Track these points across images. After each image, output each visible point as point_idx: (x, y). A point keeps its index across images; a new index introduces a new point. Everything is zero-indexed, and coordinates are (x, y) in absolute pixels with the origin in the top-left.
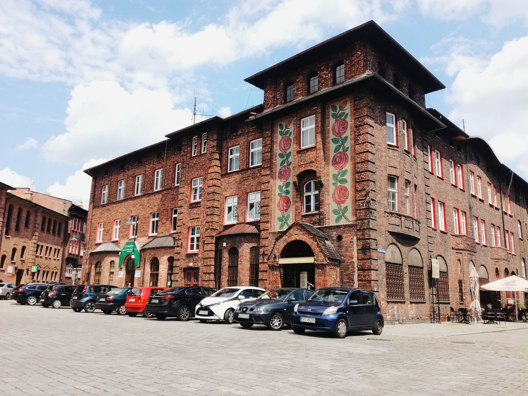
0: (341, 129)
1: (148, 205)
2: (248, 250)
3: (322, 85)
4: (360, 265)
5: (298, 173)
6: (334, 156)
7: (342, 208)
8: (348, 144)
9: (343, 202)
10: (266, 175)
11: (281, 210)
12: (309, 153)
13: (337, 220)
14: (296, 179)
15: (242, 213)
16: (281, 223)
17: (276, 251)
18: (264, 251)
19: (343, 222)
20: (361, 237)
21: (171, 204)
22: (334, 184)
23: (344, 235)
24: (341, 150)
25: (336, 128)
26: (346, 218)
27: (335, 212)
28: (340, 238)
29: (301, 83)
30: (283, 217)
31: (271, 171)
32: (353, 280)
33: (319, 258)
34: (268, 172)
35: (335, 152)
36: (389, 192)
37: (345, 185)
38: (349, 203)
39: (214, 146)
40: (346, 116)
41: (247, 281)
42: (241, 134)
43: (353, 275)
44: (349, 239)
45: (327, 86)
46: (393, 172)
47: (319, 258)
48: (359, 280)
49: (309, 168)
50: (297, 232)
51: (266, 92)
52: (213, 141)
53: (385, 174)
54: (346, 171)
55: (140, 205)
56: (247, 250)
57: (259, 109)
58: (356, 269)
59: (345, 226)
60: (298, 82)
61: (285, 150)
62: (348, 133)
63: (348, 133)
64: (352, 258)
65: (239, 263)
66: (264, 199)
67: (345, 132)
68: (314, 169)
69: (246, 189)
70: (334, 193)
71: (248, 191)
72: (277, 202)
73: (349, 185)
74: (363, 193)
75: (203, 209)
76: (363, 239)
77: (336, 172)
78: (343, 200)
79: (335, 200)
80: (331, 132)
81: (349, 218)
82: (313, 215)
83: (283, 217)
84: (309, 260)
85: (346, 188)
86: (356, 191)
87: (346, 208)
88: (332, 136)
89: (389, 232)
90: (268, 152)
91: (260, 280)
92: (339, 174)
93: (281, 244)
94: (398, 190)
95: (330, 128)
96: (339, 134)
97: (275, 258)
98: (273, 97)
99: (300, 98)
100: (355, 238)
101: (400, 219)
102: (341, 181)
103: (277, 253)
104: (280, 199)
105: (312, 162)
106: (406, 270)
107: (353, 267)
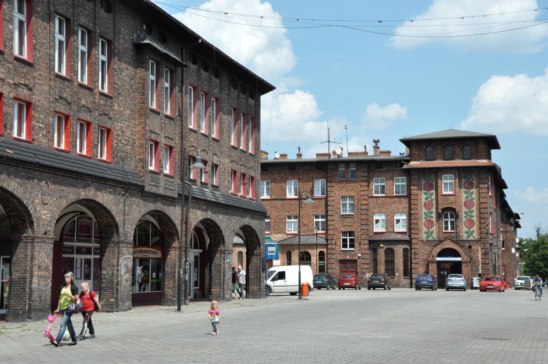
1: (282, 208)
2: (402, 250)
8: (474, 196)
9: (472, 228)
11: (427, 228)
12: (450, 197)
13: (468, 237)
14: (440, 211)
19: (471, 238)
21: (313, 211)
23: (473, 246)
24: (470, 198)
27: (466, 232)
28: (470, 247)
35: (466, 198)
37: (473, 219)
38: (475, 228)
39: (364, 176)
40: (473, 179)
44: (476, 248)
49: (451, 206)
52: (363, 172)
55: (271, 207)
58: (480, 263)
68: (454, 207)
72: (423, 222)
73: (475, 219)
74: (485, 225)
75: (355, 220)
77: (467, 210)
79: (466, 226)
81: (476, 236)
84: (459, 259)
86: (480, 223)
93: (438, 249)
97: (433, 257)
98: (418, 154)
100: (480, 248)
102: (470, 216)
107: (479, 262)
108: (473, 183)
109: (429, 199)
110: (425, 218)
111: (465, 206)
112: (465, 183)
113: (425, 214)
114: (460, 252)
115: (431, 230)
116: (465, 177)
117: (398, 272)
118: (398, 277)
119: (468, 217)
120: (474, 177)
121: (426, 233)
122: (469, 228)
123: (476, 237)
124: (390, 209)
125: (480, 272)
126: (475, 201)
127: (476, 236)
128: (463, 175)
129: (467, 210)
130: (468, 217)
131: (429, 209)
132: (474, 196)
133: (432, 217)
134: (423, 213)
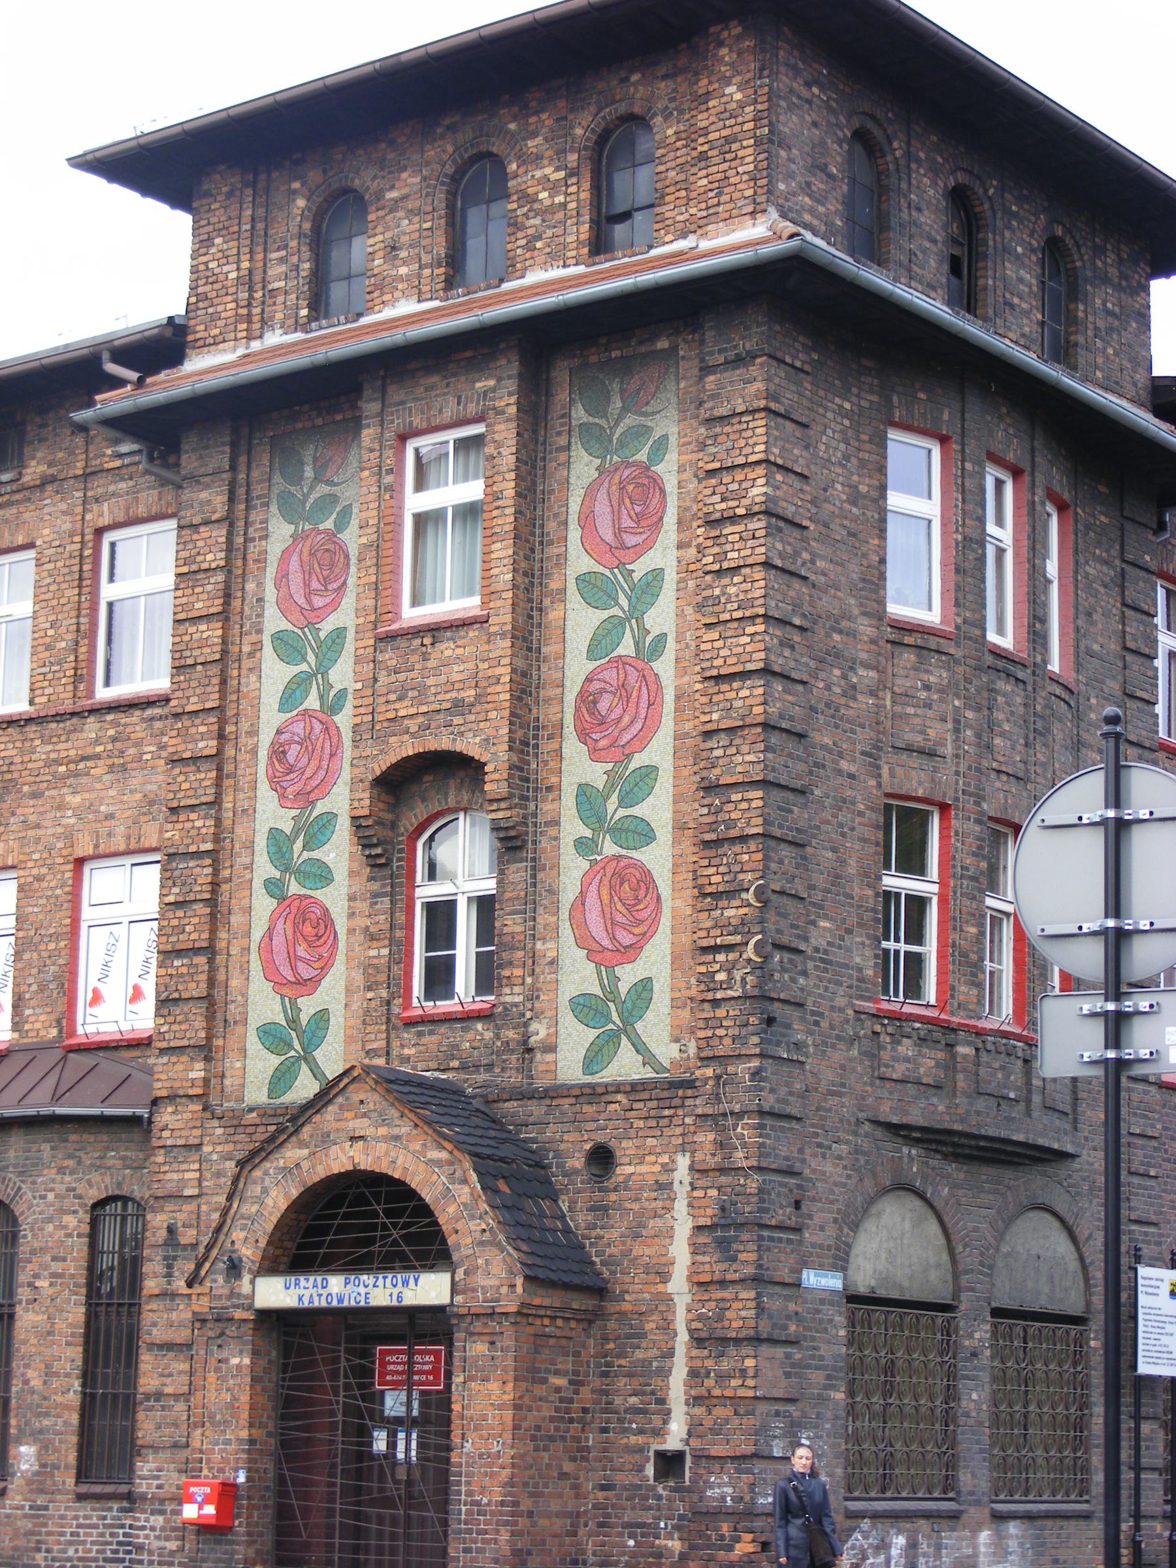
0: (627, 522)
3: (530, 247)
4: (700, 1318)
5: (379, 766)
6: (589, 680)
7: (623, 987)
8: (662, 616)
9: (630, 952)
10: (194, 759)
12: (447, 649)
13: (595, 1057)
15: (42, 988)
16: (276, 1060)
17: (238, 1235)
18: (171, 1230)
19: (625, 1065)
20: (712, 1162)
22: (581, 845)
23: (625, 1148)
24: (626, 647)
25: (602, 508)
26: (639, 1047)
28: (602, 1158)
29: (411, 212)
30: (293, 1022)
31: (221, 736)
32: (662, 1401)
33: (481, 1280)
34: (208, 746)
35: (591, 654)
36: (889, 896)
38: (656, 961)
40: (661, 446)
41: (67, 1407)
42: (46, 481)
43: (665, 1373)
44: (648, 1169)
45: (557, 256)
46: (915, 780)
47: (481, 1280)
48: (695, 1401)
49: (443, 742)
50: (360, 1125)
51: (202, 243)
53: (865, 796)
54: (650, 772)
56: (70, 1221)
57: (161, 348)
58: (683, 1337)
59: (635, 1088)
60: (395, 205)
61: (311, 616)
62: (663, 555)
63: (663, 555)
64: (665, 1277)
65: (23, 1293)
66: (177, 904)
67: (648, 545)
68: (470, 745)
69: (69, 837)
70: (583, 894)
71: (84, 847)
72: (257, 934)
73: (659, 858)
76: (722, 1171)
77: (596, 774)
78: (626, 939)
79: (584, 940)
80: (574, 534)
82: (468, 1018)
83: (293, 1022)
84: (429, 1289)
85: (647, 874)
87: (644, 987)
88: (579, 562)
89: (876, 1123)
90: (207, 617)
91: (148, 1396)
92: (610, 786)
93: (273, 1195)
94: (942, 883)
95: (575, 505)
96: (618, 553)
97: (234, 1268)
98: (248, 282)
99: (407, 307)
100: (683, 1162)
101: (950, 1046)
103: (247, 1243)
104: (273, 921)
105: (458, 706)
106: (978, 1334)
107: (667, 1327)
108: (656, 484)
109: (312, 702)
110: (269, 884)
111: (583, 735)
112: (590, 492)
113: (279, 843)
114: (446, 1215)
115: (308, 1006)
116: (597, 439)
117: (37, 1436)
118: (40, 1483)
119: (610, 848)
120: (668, 425)
121: (272, 1037)
122: (608, 957)
123: (667, 1052)
124: (49, 831)
125: (675, 1436)
126: (665, 667)
127: (662, 1039)
128: (580, 414)
129: (596, 774)
130: (610, 848)
131: (306, 799)
132: (662, 616)
133: (324, 876)
134: (261, 842)
